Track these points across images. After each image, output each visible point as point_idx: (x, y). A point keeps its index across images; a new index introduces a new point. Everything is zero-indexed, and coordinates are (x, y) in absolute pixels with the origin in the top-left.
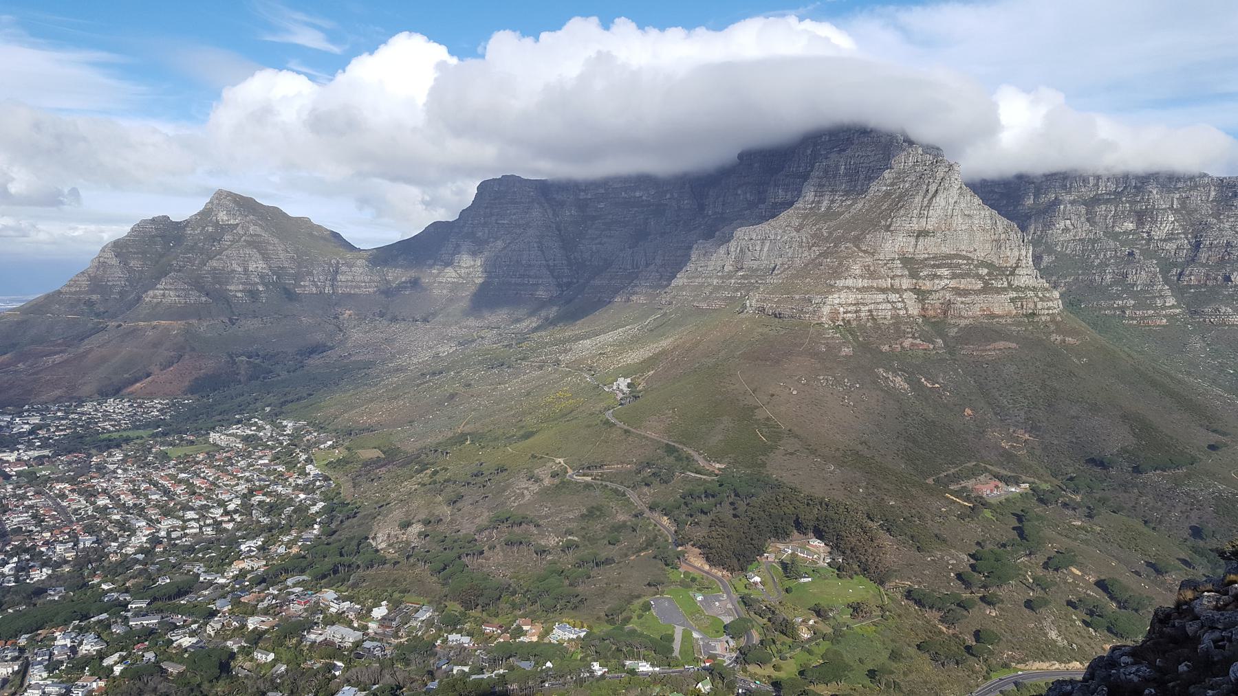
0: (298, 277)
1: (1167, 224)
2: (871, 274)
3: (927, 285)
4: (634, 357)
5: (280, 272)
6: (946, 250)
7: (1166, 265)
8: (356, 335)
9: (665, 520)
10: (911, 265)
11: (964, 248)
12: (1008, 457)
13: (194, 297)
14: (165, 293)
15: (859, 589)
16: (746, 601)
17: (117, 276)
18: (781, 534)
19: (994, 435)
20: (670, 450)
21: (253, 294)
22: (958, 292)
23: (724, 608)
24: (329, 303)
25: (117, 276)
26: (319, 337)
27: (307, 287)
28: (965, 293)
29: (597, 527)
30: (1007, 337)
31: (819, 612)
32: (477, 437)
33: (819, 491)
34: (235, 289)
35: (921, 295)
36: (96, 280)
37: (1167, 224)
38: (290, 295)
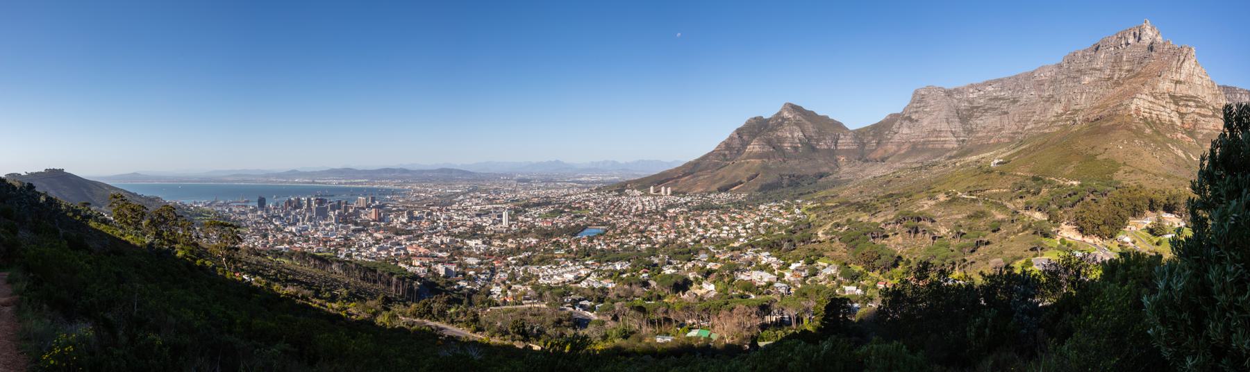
0: (818, 141)
3: (1184, 110)
5: (810, 138)
6: (1191, 93)
8: (845, 169)
13: (767, 149)
14: (754, 147)
21: (796, 148)
22: (1199, 114)
24: (831, 153)
26: (826, 169)
27: (822, 145)
28: (1205, 116)
34: (787, 145)
38: (813, 149)
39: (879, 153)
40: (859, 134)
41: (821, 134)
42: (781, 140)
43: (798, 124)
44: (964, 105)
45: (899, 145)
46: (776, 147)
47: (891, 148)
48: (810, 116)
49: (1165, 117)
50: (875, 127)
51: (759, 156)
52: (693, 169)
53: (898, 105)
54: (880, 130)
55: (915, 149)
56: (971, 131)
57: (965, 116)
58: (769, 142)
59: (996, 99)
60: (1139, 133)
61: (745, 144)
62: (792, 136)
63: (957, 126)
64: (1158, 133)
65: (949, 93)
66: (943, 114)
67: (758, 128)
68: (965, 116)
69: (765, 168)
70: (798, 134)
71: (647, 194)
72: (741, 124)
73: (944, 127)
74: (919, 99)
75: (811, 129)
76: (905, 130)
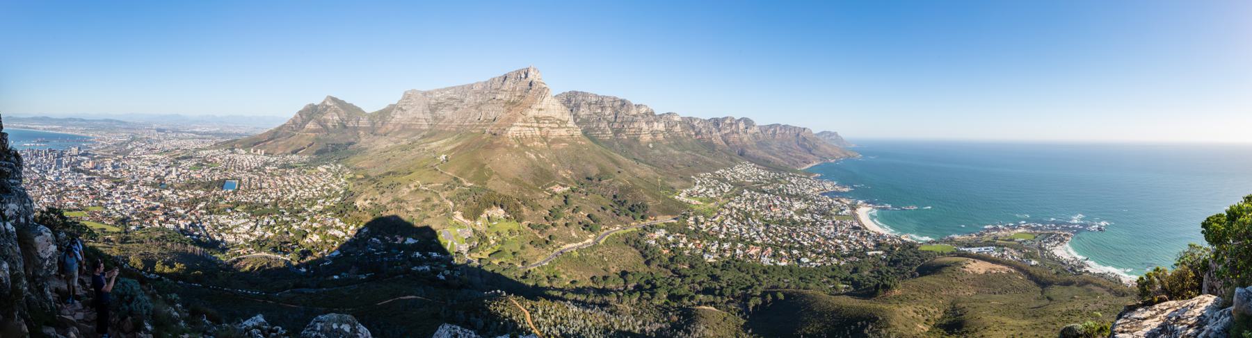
1: (608, 111)
2: (525, 121)
4: (448, 148)
7: (609, 122)
8: (364, 140)
9: (451, 203)
10: (537, 119)
11: (553, 114)
12: (564, 179)
13: (319, 127)
14: (311, 125)
15: (513, 225)
16: (474, 231)
17: (299, 121)
18: (489, 207)
19: (560, 172)
20: (455, 179)
23: (469, 233)
25: (299, 121)
27: (350, 124)
29: (428, 205)
30: (564, 141)
31: (498, 234)
32: (394, 173)
33: (503, 193)
34: (330, 125)
35: (540, 129)
36: (294, 121)
37: (608, 111)
38: (345, 127)
39: (383, 130)
40: (372, 117)
41: (349, 117)
42: (326, 121)
43: (336, 111)
44: (433, 102)
45: (395, 125)
46: (323, 124)
47: (390, 127)
48: (341, 104)
49: (529, 134)
50: (381, 112)
51: (314, 131)
52: (274, 135)
53: (395, 99)
54: (384, 114)
55: (404, 128)
56: (436, 118)
57: (433, 109)
58: (319, 123)
59: (451, 99)
60: (510, 149)
61: (305, 122)
62: (333, 118)
63: (429, 115)
64: (522, 145)
65: (425, 94)
66: (420, 108)
67: (311, 112)
68: (433, 109)
69: (317, 139)
70: (336, 118)
71: (249, 153)
72: (301, 108)
73: (421, 116)
74: (407, 97)
75: (342, 112)
76: (398, 116)
